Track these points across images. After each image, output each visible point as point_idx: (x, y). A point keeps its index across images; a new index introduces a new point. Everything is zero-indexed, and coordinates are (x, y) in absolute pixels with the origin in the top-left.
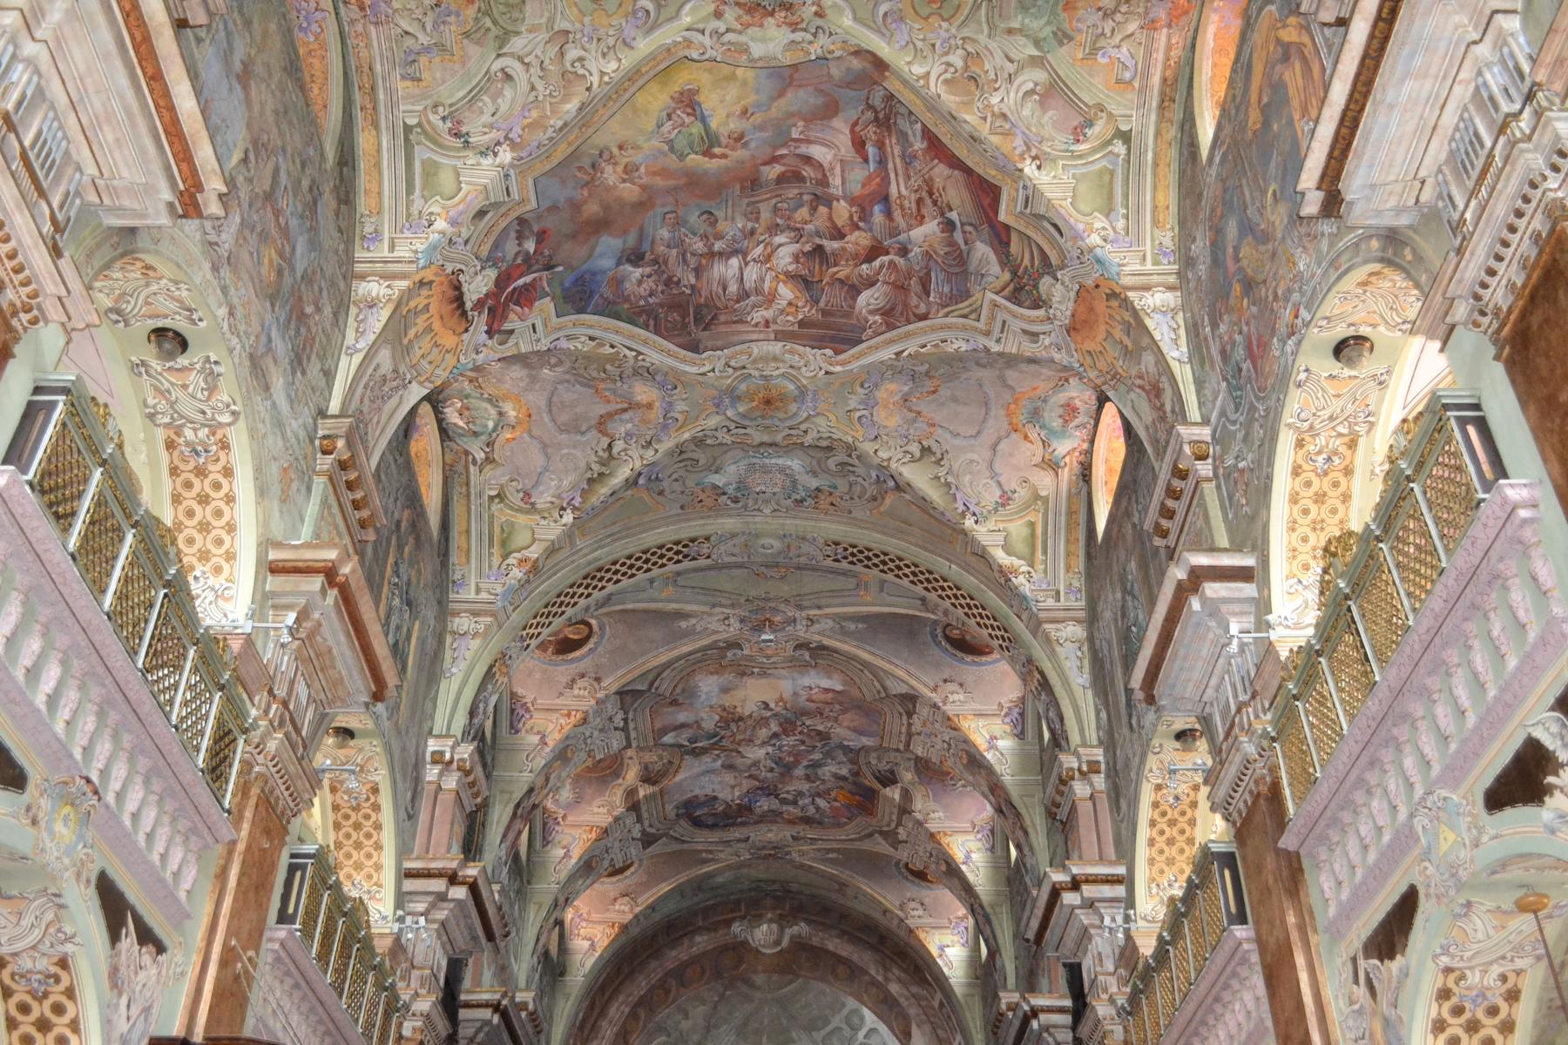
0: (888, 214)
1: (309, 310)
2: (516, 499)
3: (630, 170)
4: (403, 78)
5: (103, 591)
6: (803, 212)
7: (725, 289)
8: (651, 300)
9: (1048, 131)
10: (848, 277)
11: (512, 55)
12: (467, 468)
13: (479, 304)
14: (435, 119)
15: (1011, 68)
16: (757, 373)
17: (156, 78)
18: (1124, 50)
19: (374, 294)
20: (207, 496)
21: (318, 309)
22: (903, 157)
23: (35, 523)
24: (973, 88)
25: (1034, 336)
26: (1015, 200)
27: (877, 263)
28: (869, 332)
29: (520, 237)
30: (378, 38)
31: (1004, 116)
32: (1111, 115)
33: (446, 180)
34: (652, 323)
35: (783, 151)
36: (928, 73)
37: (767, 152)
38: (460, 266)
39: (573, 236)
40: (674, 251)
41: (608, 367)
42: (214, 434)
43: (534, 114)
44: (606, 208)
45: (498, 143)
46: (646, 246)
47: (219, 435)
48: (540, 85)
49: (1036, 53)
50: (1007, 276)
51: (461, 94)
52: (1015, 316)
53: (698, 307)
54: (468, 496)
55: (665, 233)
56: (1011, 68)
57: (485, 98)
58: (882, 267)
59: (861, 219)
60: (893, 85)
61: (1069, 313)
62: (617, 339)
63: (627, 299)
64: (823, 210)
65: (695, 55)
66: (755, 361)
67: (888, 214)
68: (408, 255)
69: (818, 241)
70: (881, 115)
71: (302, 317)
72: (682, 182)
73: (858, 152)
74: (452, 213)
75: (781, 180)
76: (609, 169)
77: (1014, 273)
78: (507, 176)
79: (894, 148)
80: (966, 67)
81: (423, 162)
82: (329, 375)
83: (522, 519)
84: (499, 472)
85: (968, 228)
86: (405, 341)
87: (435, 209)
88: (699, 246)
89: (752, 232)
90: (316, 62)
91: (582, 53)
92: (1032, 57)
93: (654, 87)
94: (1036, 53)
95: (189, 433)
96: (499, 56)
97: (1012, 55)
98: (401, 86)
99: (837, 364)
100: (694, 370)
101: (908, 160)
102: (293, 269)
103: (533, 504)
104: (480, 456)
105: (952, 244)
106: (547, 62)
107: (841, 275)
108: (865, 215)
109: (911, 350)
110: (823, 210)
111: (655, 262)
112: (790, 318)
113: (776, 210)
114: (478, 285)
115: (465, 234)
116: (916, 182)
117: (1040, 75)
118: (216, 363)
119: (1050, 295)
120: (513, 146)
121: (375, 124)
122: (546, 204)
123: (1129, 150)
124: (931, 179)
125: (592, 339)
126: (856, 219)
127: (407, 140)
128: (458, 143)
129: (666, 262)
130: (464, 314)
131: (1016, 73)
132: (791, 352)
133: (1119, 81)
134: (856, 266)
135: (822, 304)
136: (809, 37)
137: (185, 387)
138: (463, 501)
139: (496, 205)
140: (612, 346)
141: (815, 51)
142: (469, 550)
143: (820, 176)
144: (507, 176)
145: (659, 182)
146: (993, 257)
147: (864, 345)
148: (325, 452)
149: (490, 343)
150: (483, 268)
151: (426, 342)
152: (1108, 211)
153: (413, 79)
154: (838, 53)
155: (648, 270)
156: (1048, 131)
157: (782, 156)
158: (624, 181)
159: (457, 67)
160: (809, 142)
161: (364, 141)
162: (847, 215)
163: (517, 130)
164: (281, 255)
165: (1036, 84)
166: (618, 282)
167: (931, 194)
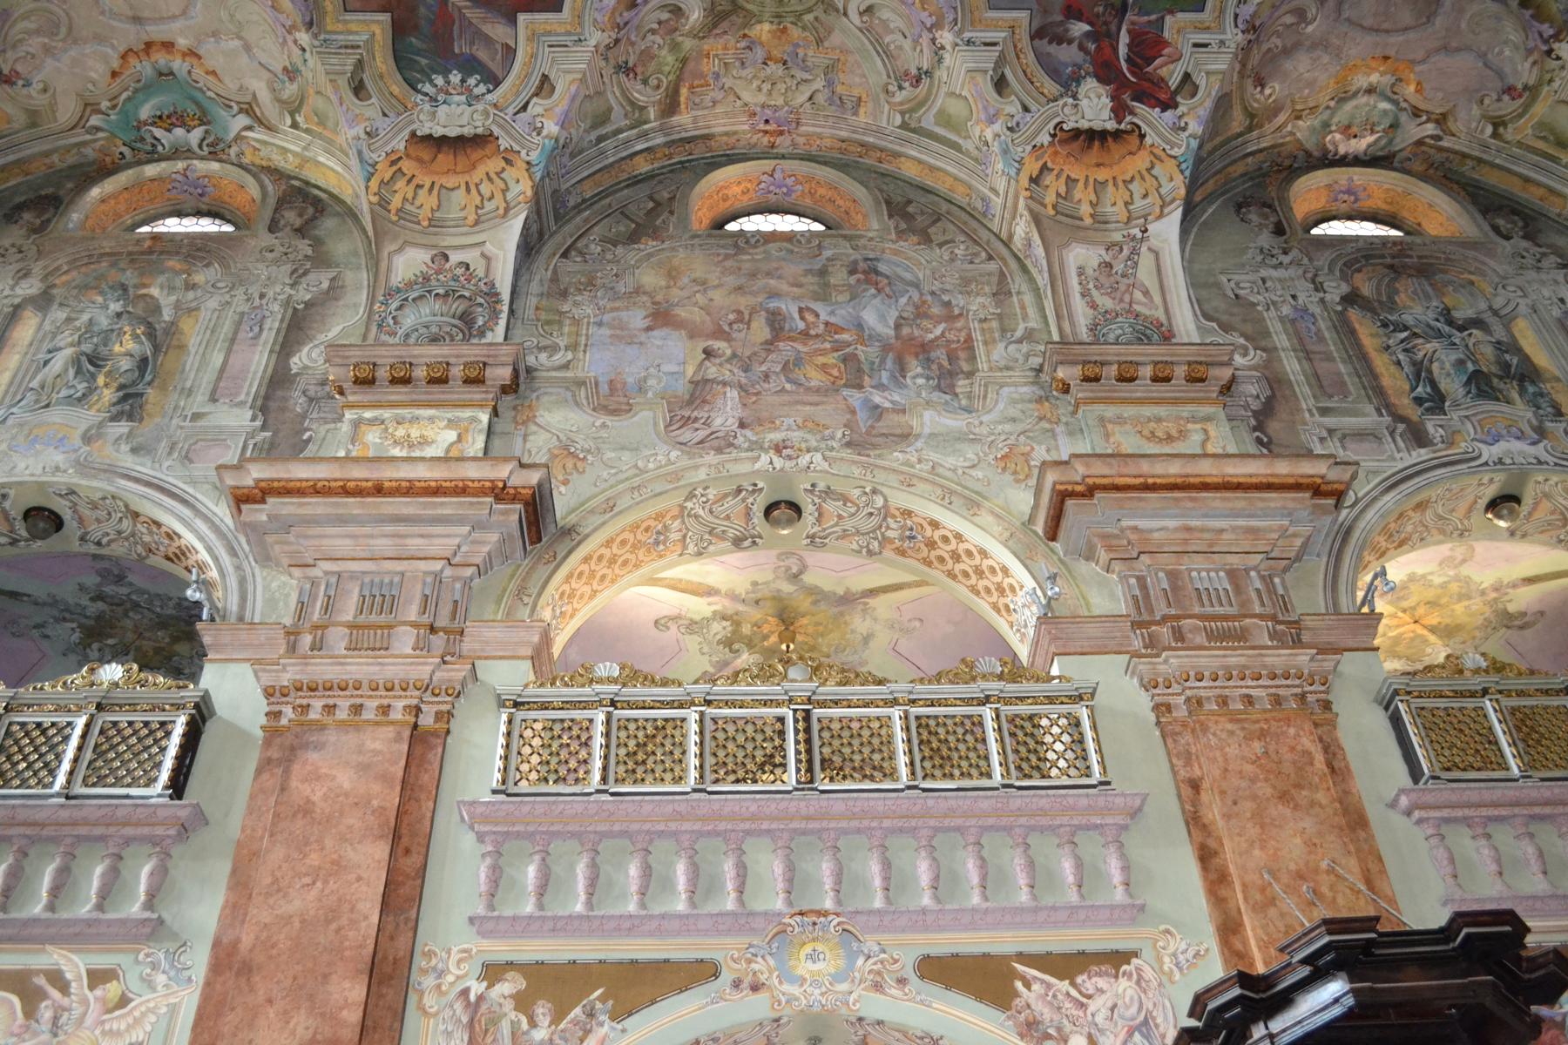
2: (1508, 106)
4: (856, 114)
12: (1441, 149)
13: (1119, 111)
14: (900, 97)
29: (1061, 39)
33: (956, 108)
45: (933, 40)
51: (879, 63)
54: (1480, 161)
74: (983, 117)
78: (969, 42)
81: (937, 124)
83: (1540, 109)
84: (1462, 114)
86: (1088, 221)
90: (821, 191)
96: (845, 14)
98: (863, 118)
103: (1526, 87)
104: (1430, 128)
120: (937, 25)
121: (897, 155)
127: (914, 131)
128: (925, 81)
138: (1486, 169)
139: (1001, 61)
142: (1551, 191)
144: (969, 42)
149: (1182, 109)
150: (1074, 97)
153: (859, 105)
159: (851, 59)
163: (924, 15)
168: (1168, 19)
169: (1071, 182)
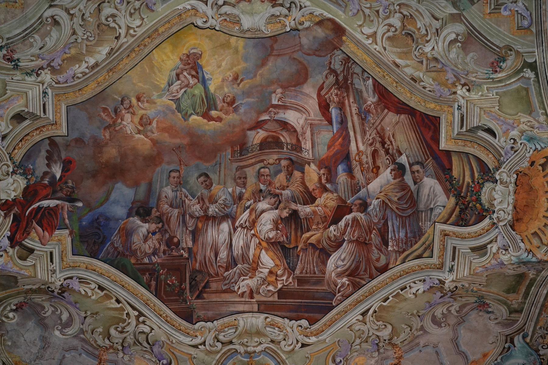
0: (350, 171)
3: (144, 122)
6: (281, 178)
7: (216, 255)
8: (154, 259)
9: (472, 66)
10: (319, 241)
11: (61, 7)
15: (437, 24)
16: (241, 349)
18: (520, 4)
22: (359, 114)
24: (410, 41)
25: (481, 250)
26: (452, 124)
27: (342, 223)
28: (338, 296)
29: (49, 158)
31: (436, 59)
32: (518, 53)
34: (153, 283)
35: (265, 117)
36: (375, 33)
37: (251, 118)
39: (94, 175)
40: (176, 211)
41: (113, 332)
43: (73, 51)
44: (123, 156)
45: (42, 68)
46: (153, 202)
48: (80, 32)
49: (455, 11)
50: (453, 200)
52: (463, 238)
53: (194, 272)
55: (168, 191)
56: (437, 24)
57: (36, 36)
58: (346, 225)
59: (328, 181)
60: (349, 48)
61: (511, 207)
62: (123, 294)
63: (134, 253)
64: (297, 174)
65: (200, 23)
66: (240, 336)
67: (350, 171)
69: (293, 206)
70: (341, 78)
72: (186, 141)
73: (324, 114)
75: (264, 145)
76: (128, 117)
77: (458, 196)
78: (45, 93)
79: (352, 108)
80: (404, 27)
85: (416, 167)
88: (196, 208)
89: (240, 198)
91: (115, 11)
92: (452, 15)
93: (167, 47)
94: (455, 11)
96: (51, 6)
97: (437, 15)
99: (312, 334)
100: (187, 340)
101: (363, 115)
105: (404, 187)
106: (87, 15)
107: (313, 240)
108: (331, 176)
109: (375, 307)
110: (297, 174)
111: (160, 219)
112: (271, 288)
113: (259, 175)
116: (371, 134)
117: (460, 28)
119: (492, 200)
122: (75, 135)
123: (537, 74)
124: (383, 129)
125: (101, 288)
126: (324, 181)
128: (10, 65)
129: (168, 221)
131: (442, 27)
132: (273, 325)
133: (519, 28)
134: (326, 228)
135: (297, 272)
136: (285, 11)
139: (34, 117)
140: (118, 301)
141: (289, 23)
143: (294, 141)
144: (45, 93)
145: (166, 138)
146: (439, 188)
147: (334, 311)
149: (10, 250)
150: (14, 172)
152: (530, 111)
154: (307, 24)
155: (153, 227)
156: (472, 66)
157: (265, 122)
158: (139, 132)
159: (17, 11)
160: (285, 107)
162: (315, 178)
165: (458, 35)
166: (128, 233)
167: (383, 143)
168: (67, 231)
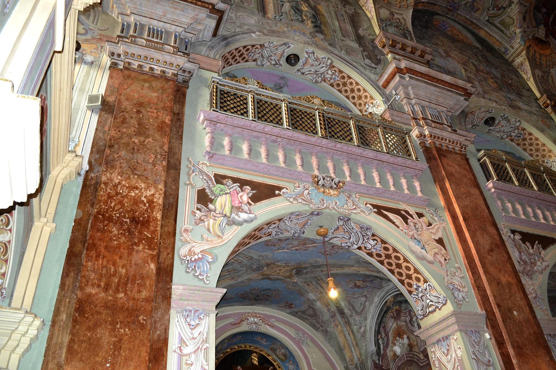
1: (510, 82)
4: (475, 12)
5: (532, 187)
13: (547, 36)
14: (491, 12)
17: (438, 81)
19: (520, 62)
20: (531, 143)
21: (512, 79)
23: (506, 187)
30: (462, 12)
33: (508, 20)
38: (532, 34)
42: (519, 129)
47: (520, 129)
68: (518, 45)
71: (510, 85)
74: (518, 25)
81: (499, 23)
82: (530, 90)
86: (538, 63)
87: (513, 29)
90: (455, 32)
95: (513, 134)
98: (476, 15)
102: (498, 78)
114: (541, 33)
115: (525, 26)
118: (504, 115)
127: (490, 23)
128: (502, 10)
130: (545, 42)
137: (503, 126)
139: (526, 12)
144: (521, 4)
148: (547, 107)
151: (544, 58)
153: (477, 10)
161: (482, 34)
164: (492, 78)
169: (535, 51)
